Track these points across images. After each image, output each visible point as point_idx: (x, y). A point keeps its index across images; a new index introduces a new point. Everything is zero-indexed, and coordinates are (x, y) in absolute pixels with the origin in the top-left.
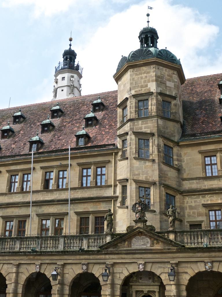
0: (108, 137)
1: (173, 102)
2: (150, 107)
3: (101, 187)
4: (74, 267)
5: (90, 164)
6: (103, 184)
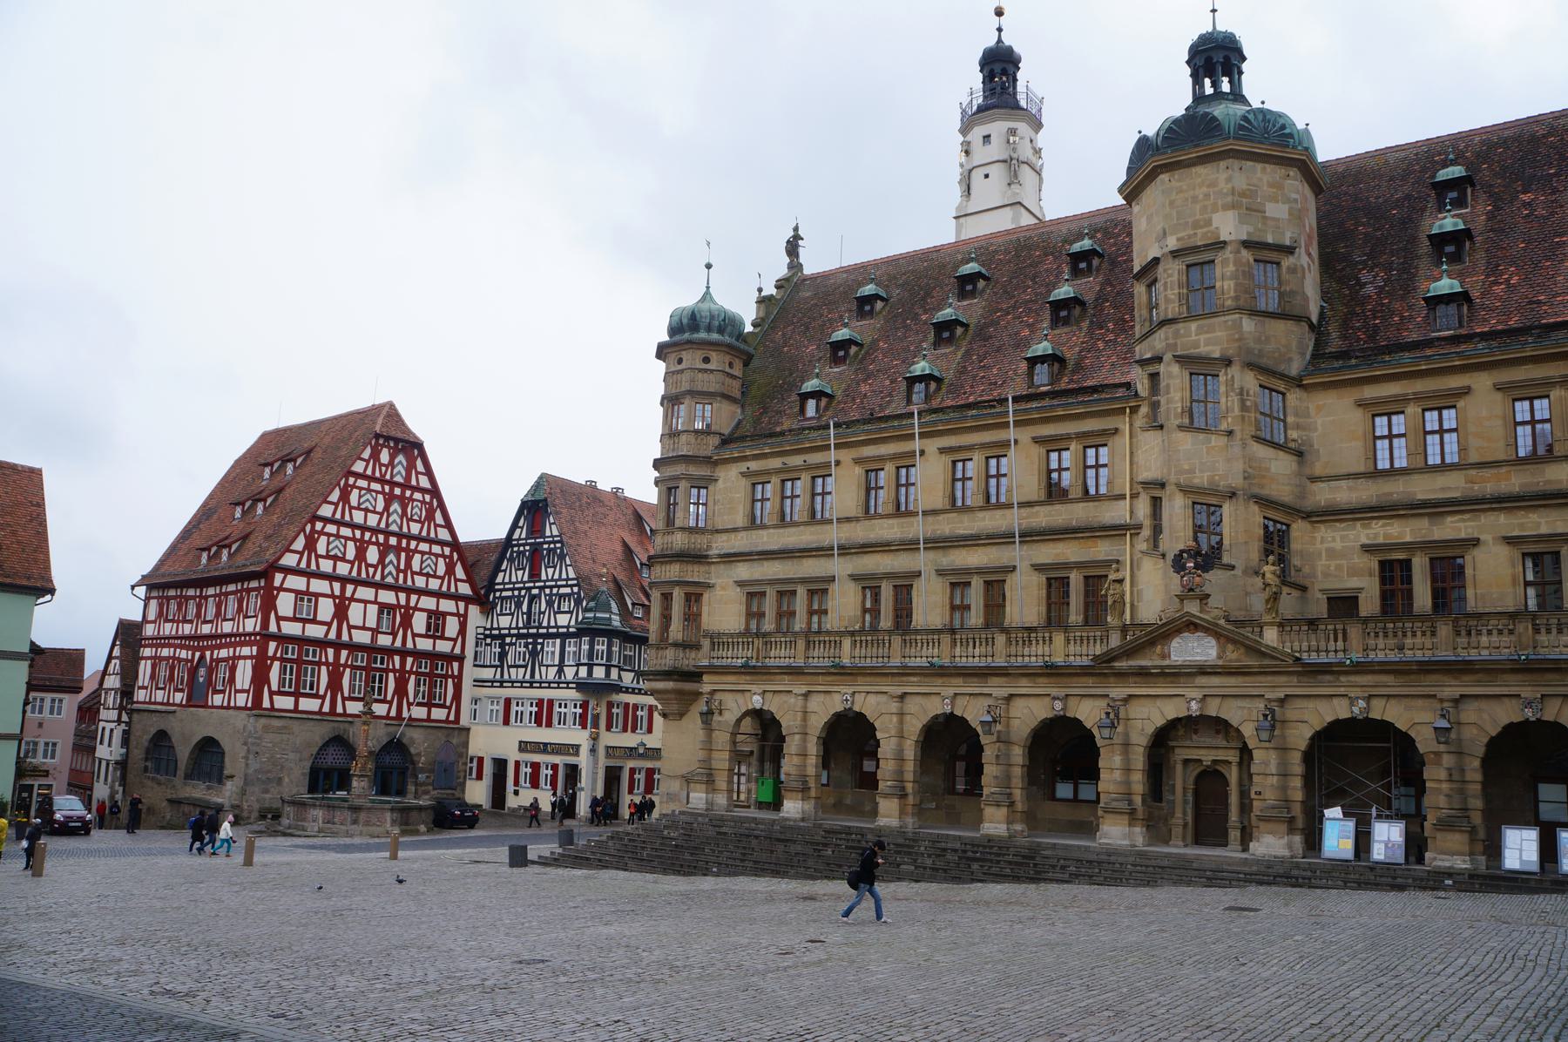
0: (1114, 359)
1: (1287, 262)
2: (1218, 284)
3: (1098, 498)
4: (1032, 703)
5: (1068, 438)
6: (1103, 490)
